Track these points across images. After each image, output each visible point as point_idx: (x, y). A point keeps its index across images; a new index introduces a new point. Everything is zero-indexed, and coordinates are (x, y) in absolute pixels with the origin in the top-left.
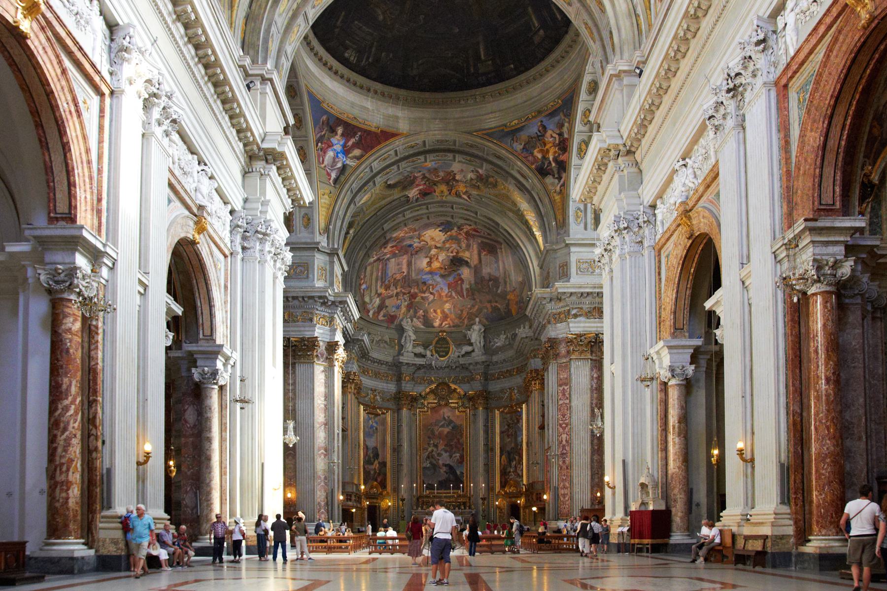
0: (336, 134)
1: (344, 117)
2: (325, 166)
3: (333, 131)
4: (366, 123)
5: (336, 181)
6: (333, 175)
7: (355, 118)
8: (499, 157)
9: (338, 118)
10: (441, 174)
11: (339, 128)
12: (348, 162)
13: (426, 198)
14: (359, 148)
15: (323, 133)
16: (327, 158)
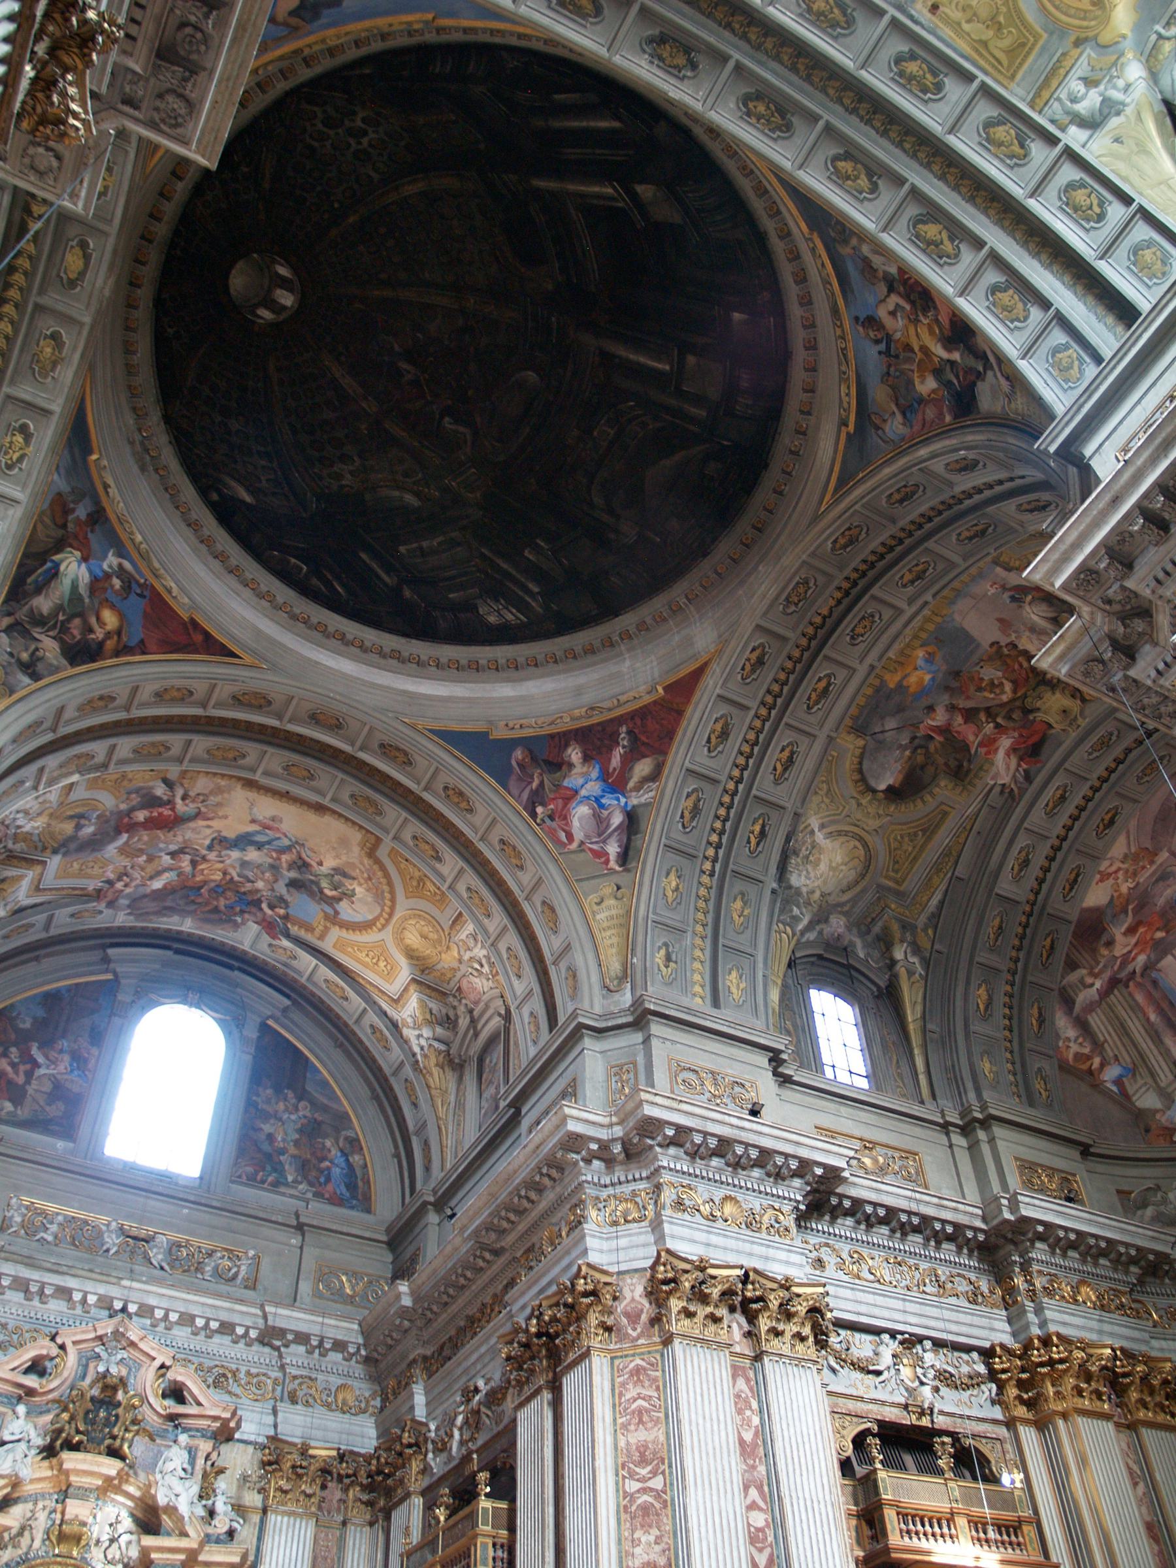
0: (571, 766)
1: (566, 724)
2: (582, 843)
3: (558, 765)
4: (623, 698)
5: (624, 857)
6: (613, 849)
7: (592, 709)
8: (907, 495)
9: (552, 736)
10: (990, 673)
11: (569, 750)
12: (634, 801)
13: (1043, 757)
14: (644, 756)
15: (535, 785)
16: (576, 823)
